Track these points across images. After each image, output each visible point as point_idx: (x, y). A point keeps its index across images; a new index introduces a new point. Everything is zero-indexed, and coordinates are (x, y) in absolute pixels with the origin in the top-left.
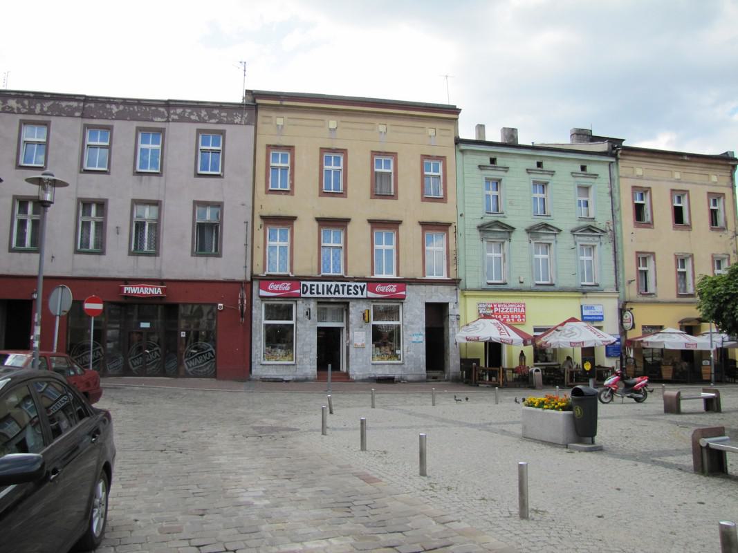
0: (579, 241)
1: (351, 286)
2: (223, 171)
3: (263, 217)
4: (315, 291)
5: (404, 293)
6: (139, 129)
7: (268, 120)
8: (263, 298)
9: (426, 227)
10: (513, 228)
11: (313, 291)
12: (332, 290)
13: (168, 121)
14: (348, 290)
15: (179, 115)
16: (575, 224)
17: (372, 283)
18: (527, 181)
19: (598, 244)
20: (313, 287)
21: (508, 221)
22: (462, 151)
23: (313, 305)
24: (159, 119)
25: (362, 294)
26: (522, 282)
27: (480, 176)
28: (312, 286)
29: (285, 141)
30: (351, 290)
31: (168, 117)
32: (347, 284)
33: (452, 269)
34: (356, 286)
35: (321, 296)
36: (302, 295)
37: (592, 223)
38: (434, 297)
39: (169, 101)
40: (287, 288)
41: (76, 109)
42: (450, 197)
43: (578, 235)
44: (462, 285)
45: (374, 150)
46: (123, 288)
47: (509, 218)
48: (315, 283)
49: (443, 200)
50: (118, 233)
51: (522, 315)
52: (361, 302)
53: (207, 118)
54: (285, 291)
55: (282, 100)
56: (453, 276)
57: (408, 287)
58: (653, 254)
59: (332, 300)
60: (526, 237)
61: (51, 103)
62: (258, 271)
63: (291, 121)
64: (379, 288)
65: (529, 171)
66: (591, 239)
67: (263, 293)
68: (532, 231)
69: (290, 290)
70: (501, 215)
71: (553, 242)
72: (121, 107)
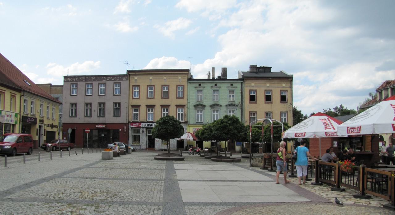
0: (229, 109)
2: (120, 94)
6: (99, 83)
7: (132, 78)
8: (132, 128)
12: (150, 125)
13: (106, 81)
16: (227, 103)
19: (235, 109)
21: (204, 103)
22: (190, 83)
23: (145, 130)
24: (104, 80)
27: (195, 90)
29: (137, 84)
33: (185, 118)
35: (147, 127)
37: (233, 103)
39: (106, 75)
40: (138, 125)
41: (84, 79)
42: (186, 97)
43: (228, 107)
44: (188, 123)
46: (96, 126)
47: (204, 102)
48: (145, 123)
49: (183, 98)
55: (136, 72)
56: (185, 121)
58: (256, 112)
60: (210, 108)
61: (78, 78)
62: (130, 121)
65: (212, 87)
66: (233, 108)
67: (131, 126)
68: (212, 106)
71: (219, 110)
72: (95, 78)
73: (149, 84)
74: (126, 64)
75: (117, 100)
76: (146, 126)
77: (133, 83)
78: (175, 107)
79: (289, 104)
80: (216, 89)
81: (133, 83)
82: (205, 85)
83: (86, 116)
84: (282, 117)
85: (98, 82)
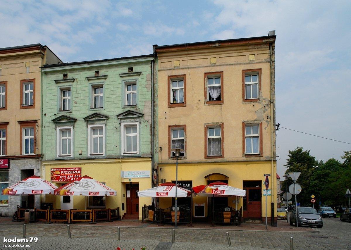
0: (124, 122)
9: (22, 125)
10: (76, 120)
16: (121, 111)
21: (73, 115)
38: (25, 167)
42: (37, 104)
43: (121, 119)
47: (74, 113)
49: (32, 106)
65: (89, 79)
68: (88, 119)
70: (69, 111)
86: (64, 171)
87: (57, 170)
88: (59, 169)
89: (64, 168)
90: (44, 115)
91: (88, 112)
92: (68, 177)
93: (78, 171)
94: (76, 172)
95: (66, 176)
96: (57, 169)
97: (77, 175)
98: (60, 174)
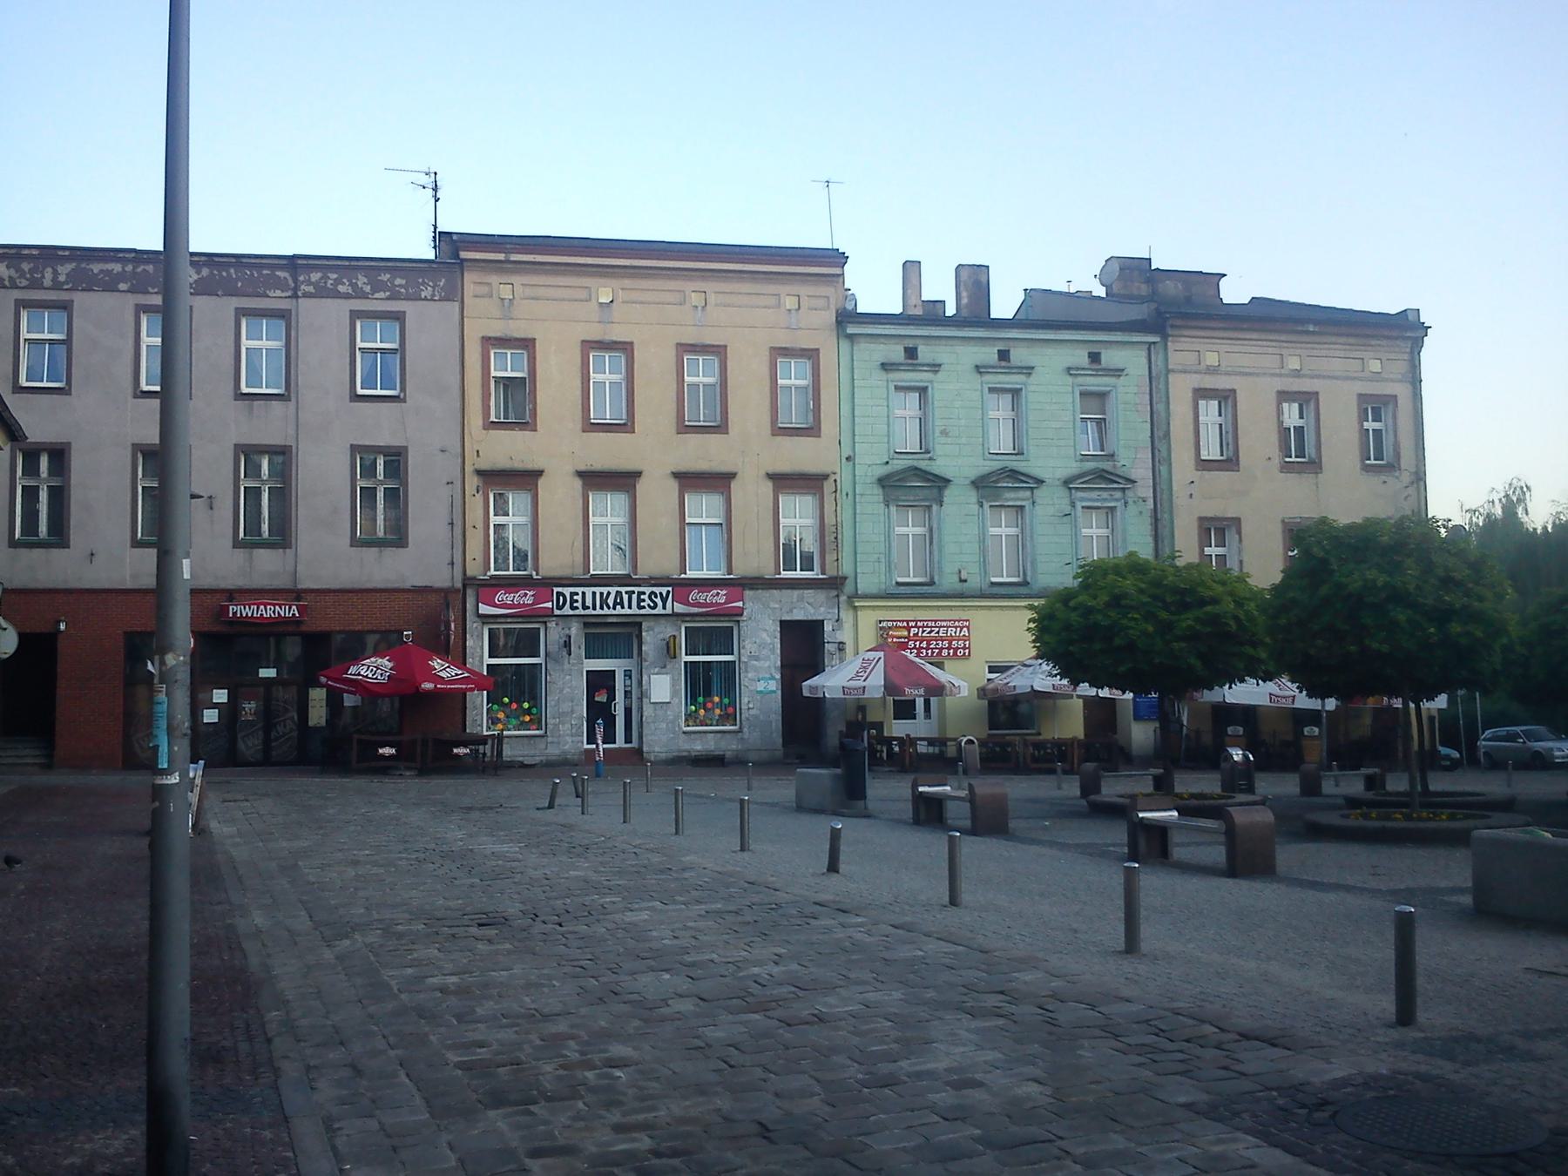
0: (1082, 499)
1: (644, 593)
2: (403, 389)
3: (479, 473)
4: (579, 604)
5: (740, 604)
6: (241, 313)
8: (485, 619)
11: (575, 605)
12: (611, 602)
13: (295, 296)
14: (640, 600)
15: (315, 285)
16: (1072, 468)
17: (682, 587)
18: (972, 387)
20: (575, 597)
21: (940, 467)
22: (851, 337)
23: (575, 630)
24: (278, 293)
25: (664, 608)
26: (965, 581)
28: (572, 594)
30: (644, 600)
31: (296, 289)
32: (636, 589)
33: (830, 558)
34: (652, 593)
36: (557, 612)
37: (1107, 465)
39: (294, 258)
41: (122, 277)
42: (827, 426)
44: (848, 588)
45: (683, 342)
47: (938, 462)
48: (579, 590)
49: (812, 430)
50: (211, 508)
51: (968, 638)
52: (663, 621)
53: (368, 289)
54: (524, 605)
56: (831, 572)
57: (748, 593)
58: (1237, 522)
59: (610, 620)
60: (972, 496)
62: (473, 570)
63: (529, 292)
64: (694, 595)
66: (1105, 495)
67: (484, 609)
68: (985, 485)
69: (533, 604)
72: (205, 272)
73: (595, 333)
74: (430, 192)
75: (382, 428)
76: (585, 607)
77: (483, 318)
78: (674, 485)
79: (1406, 478)
80: (1001, 378)
81: (483, 318)
82: (939, 353)
83: (250, 541)
84: (1207, 550)
85: (236, 302)
86: (921, 629)
87: (900, 624)
88: (903, 621)
89: (920, 621)
90: (844, 460)
91: (981, 462)
92: (931, 646)
93: (962, 628)
94: (955, 633)
95: (925, 642)
96: (900, 621)
97: (958, 640)
98: (908, 637)
